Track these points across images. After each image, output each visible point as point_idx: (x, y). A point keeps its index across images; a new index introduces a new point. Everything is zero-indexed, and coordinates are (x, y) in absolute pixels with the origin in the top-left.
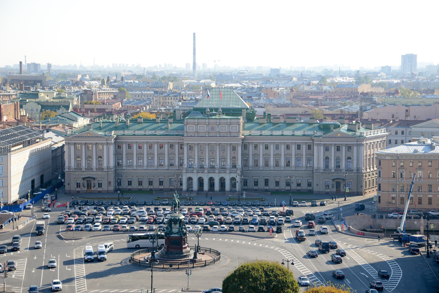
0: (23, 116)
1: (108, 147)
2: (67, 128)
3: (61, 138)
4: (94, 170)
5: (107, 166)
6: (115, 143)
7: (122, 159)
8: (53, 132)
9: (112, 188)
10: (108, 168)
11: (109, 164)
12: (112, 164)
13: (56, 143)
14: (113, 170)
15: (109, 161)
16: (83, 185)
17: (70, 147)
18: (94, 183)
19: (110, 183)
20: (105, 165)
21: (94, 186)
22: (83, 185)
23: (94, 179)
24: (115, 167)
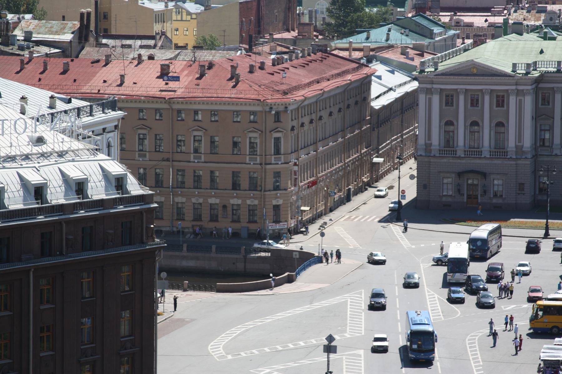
0: (307, 24)
1: (520, 100)
2: (412, 53)
3: (400, 77)
4: (486, 154)
5: (516, 146)
6: (536, 91)
7: (551, 129)
8: (381, 62)
9: (526, 199)
10: (519, 149)
11: (520, 141)
12: (527, 142)
13: (391, 89)
14: (529, 156)
15: (521, 133)
16: (459, 191)
17: (430, 99)
18: (484, 186)
19: (521, 186)
20: (512, 143)
21: (485, 192)
22: (459, 191)
23: (484, 175)
24: (535, 147)
